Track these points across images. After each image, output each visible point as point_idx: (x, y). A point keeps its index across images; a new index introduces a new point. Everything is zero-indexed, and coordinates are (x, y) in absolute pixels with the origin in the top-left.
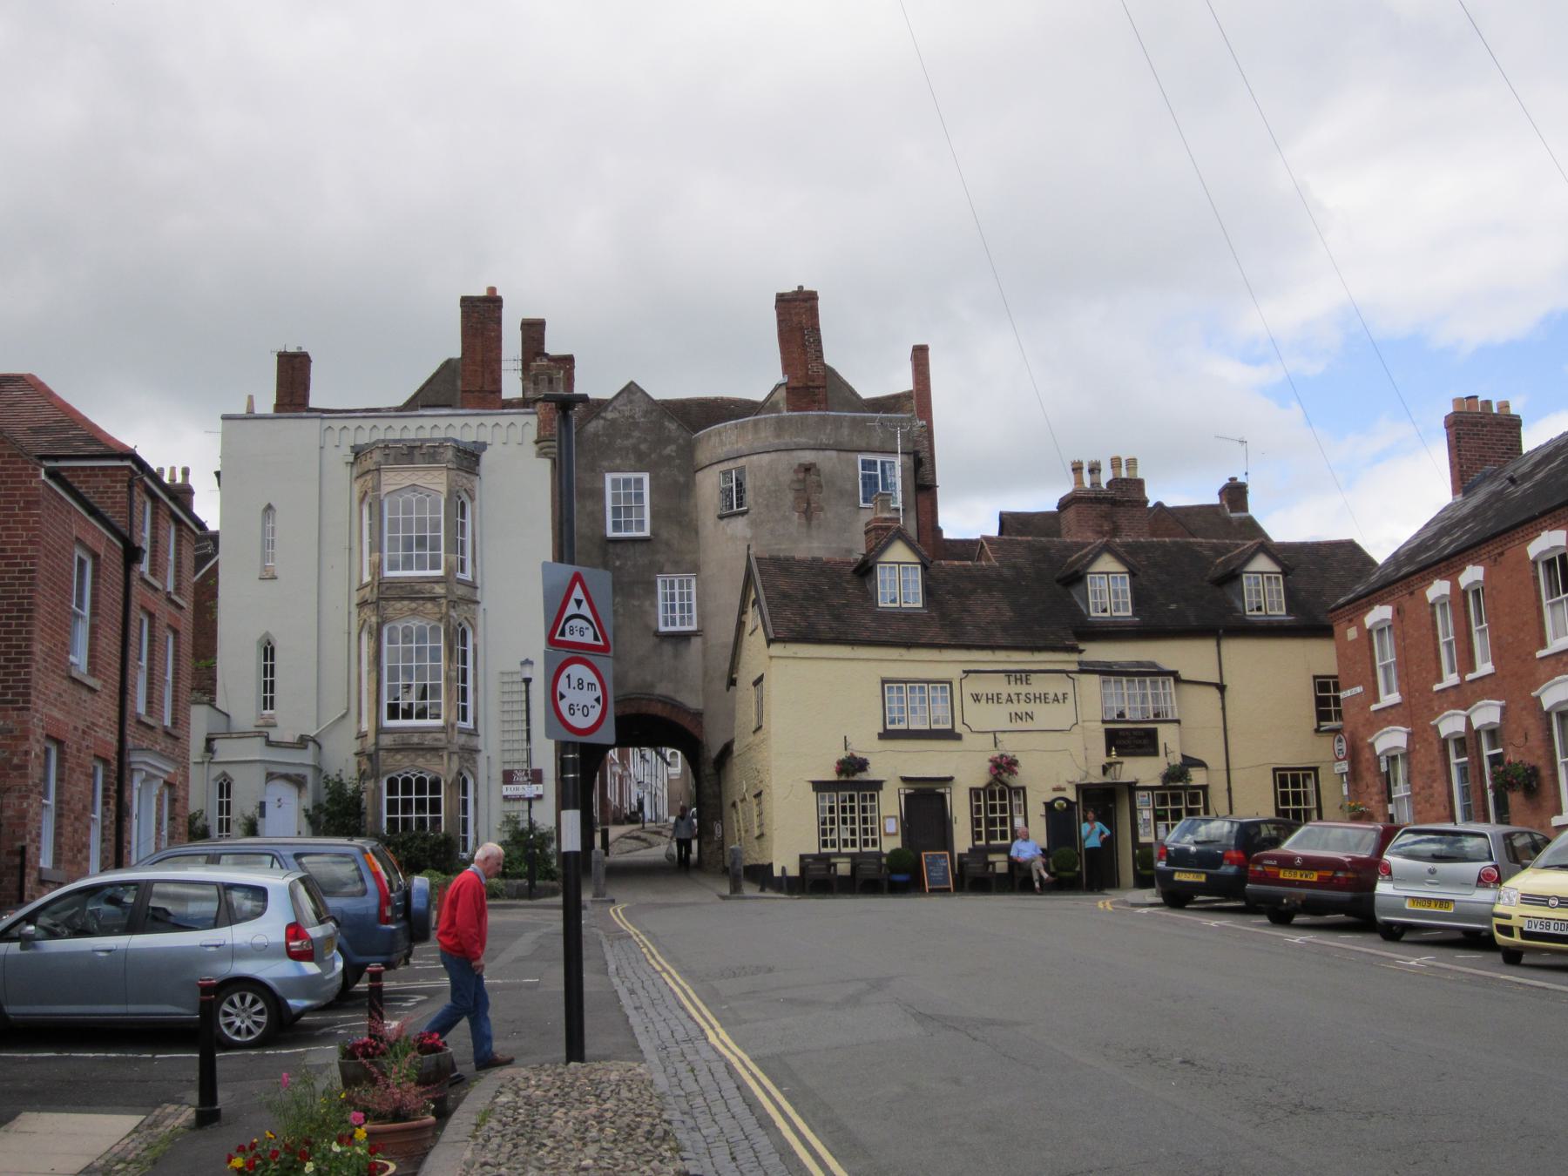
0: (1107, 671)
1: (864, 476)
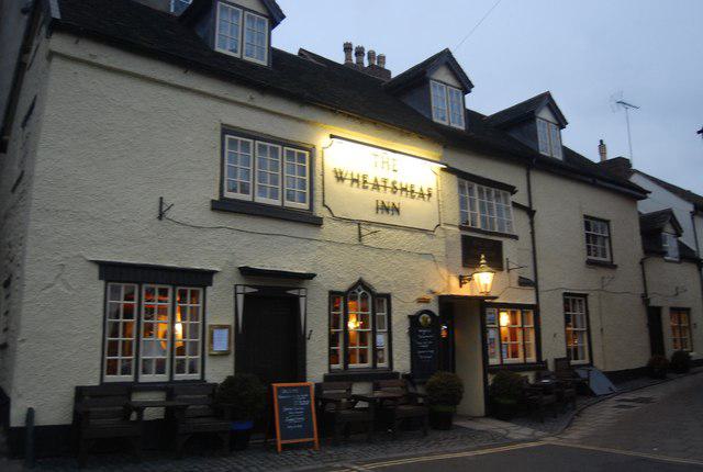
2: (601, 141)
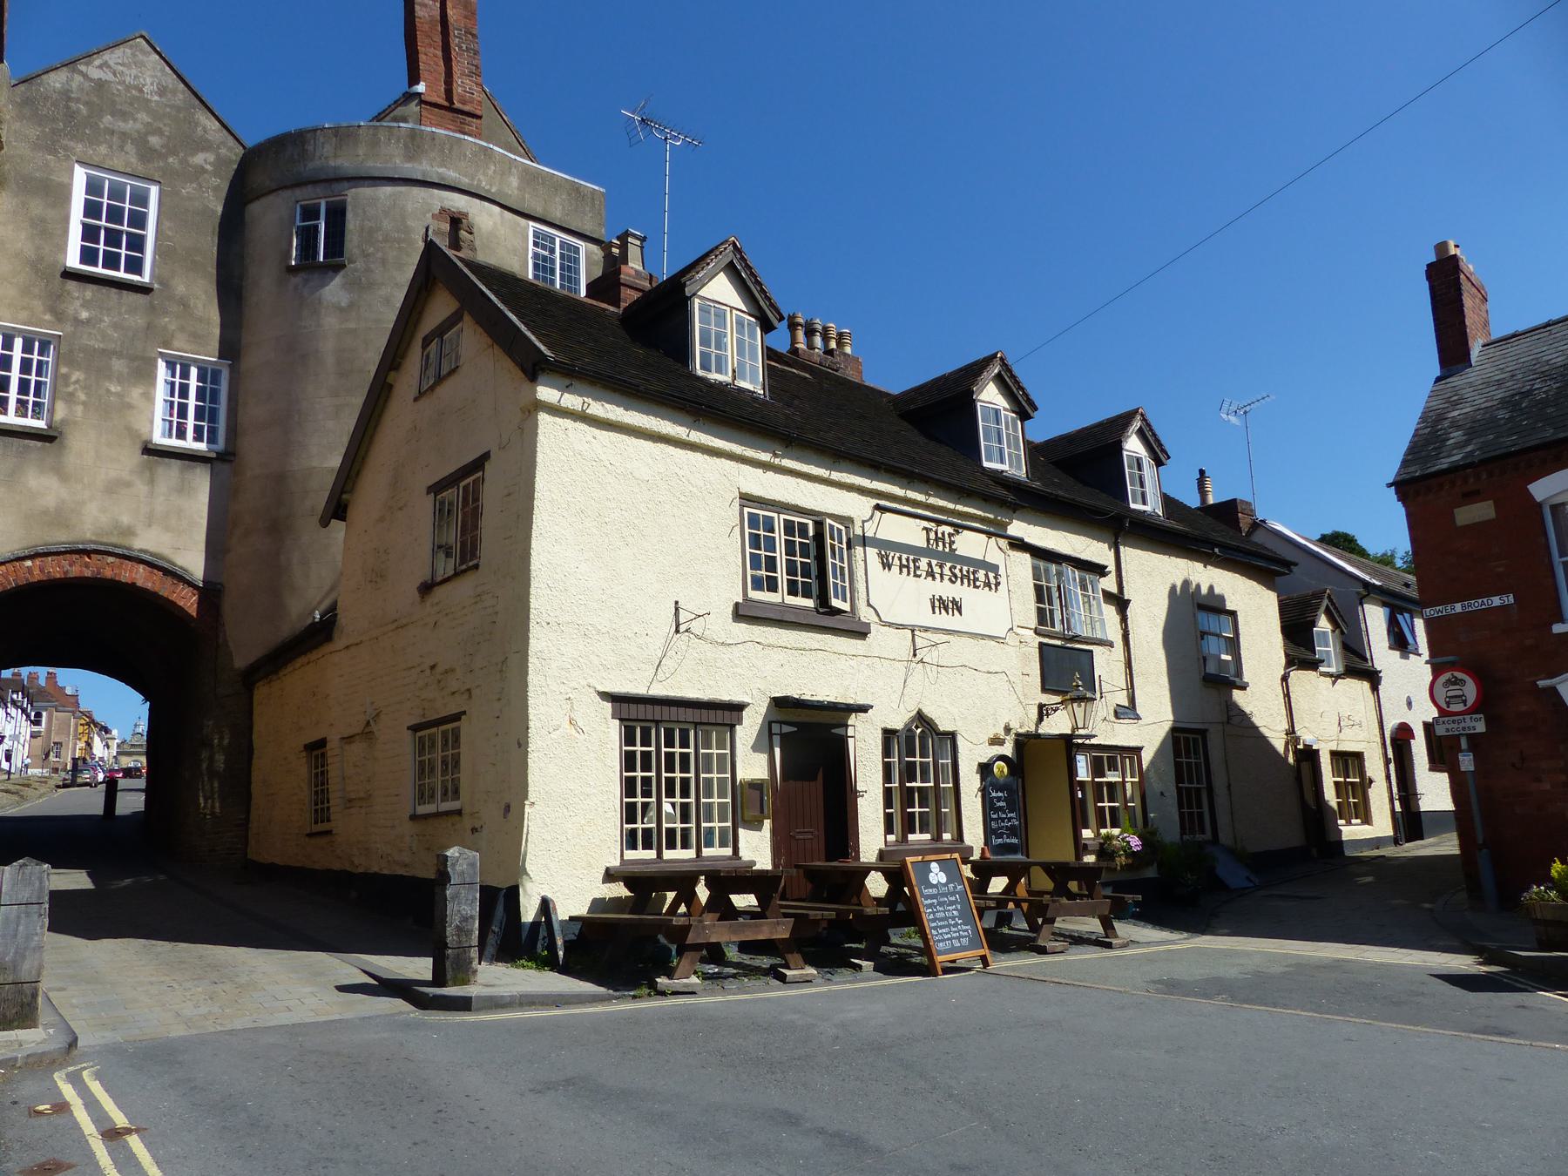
0: (1038, 553)
1: (536, 256)
2: (1202, 472)
